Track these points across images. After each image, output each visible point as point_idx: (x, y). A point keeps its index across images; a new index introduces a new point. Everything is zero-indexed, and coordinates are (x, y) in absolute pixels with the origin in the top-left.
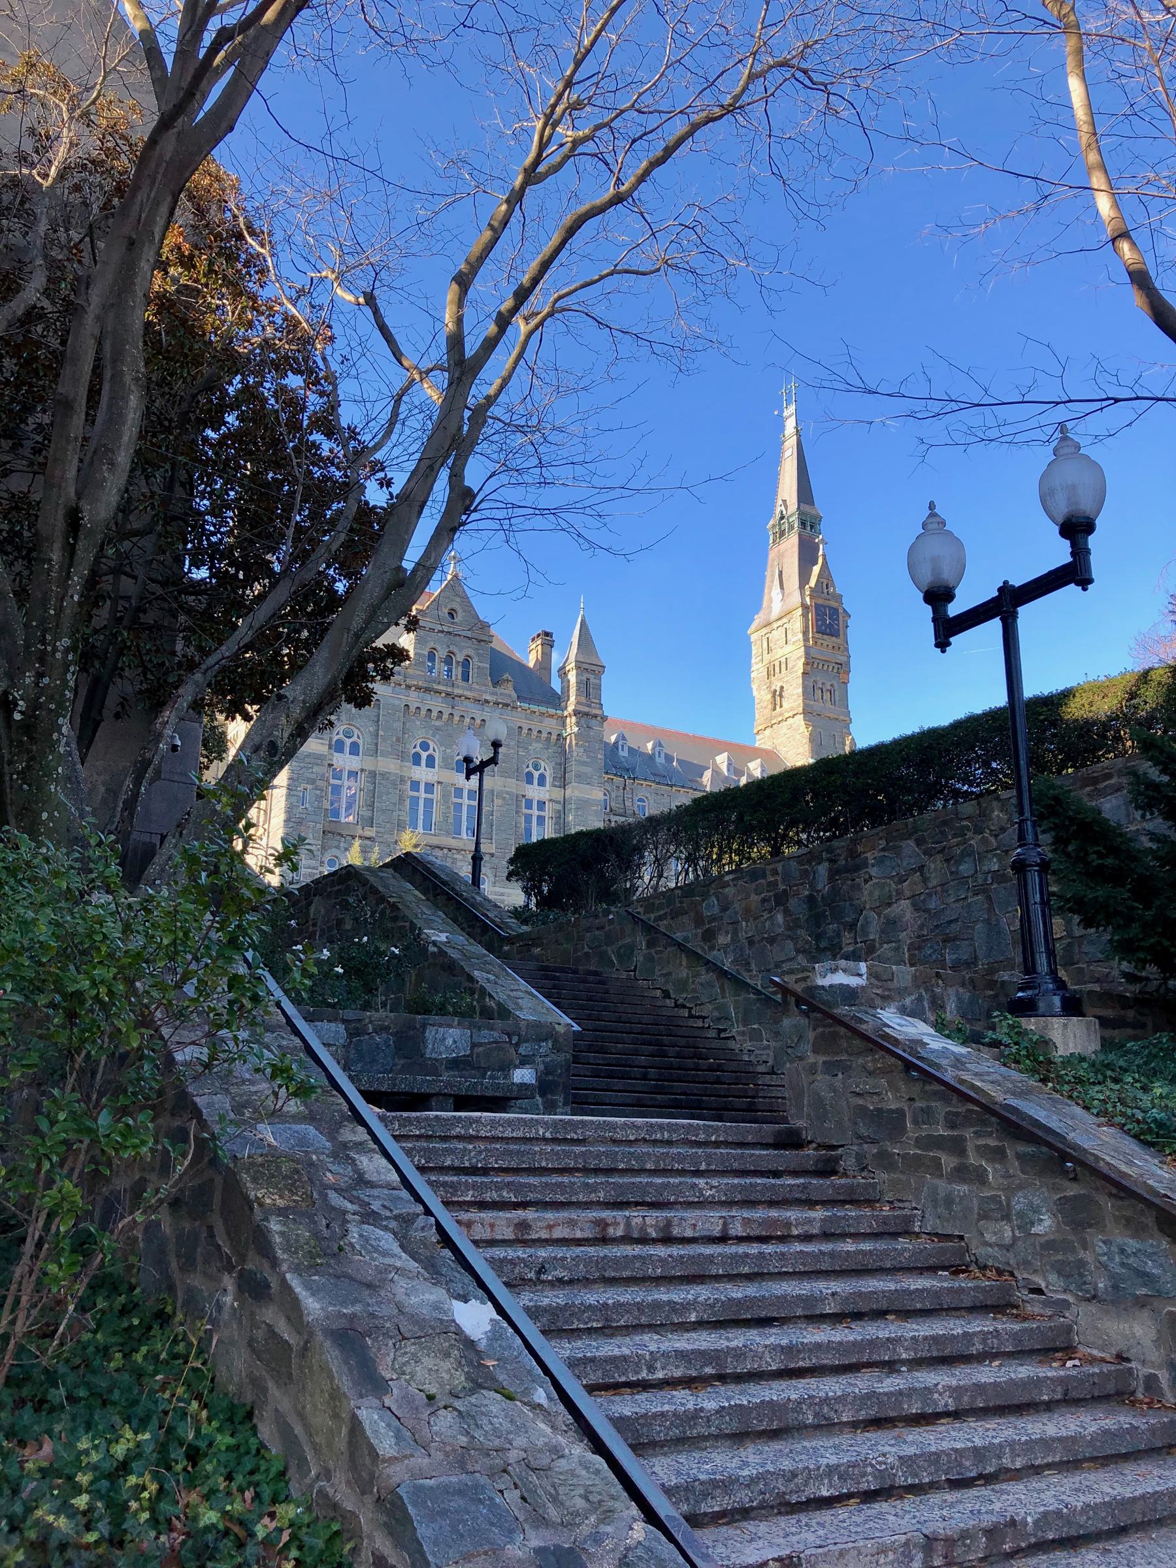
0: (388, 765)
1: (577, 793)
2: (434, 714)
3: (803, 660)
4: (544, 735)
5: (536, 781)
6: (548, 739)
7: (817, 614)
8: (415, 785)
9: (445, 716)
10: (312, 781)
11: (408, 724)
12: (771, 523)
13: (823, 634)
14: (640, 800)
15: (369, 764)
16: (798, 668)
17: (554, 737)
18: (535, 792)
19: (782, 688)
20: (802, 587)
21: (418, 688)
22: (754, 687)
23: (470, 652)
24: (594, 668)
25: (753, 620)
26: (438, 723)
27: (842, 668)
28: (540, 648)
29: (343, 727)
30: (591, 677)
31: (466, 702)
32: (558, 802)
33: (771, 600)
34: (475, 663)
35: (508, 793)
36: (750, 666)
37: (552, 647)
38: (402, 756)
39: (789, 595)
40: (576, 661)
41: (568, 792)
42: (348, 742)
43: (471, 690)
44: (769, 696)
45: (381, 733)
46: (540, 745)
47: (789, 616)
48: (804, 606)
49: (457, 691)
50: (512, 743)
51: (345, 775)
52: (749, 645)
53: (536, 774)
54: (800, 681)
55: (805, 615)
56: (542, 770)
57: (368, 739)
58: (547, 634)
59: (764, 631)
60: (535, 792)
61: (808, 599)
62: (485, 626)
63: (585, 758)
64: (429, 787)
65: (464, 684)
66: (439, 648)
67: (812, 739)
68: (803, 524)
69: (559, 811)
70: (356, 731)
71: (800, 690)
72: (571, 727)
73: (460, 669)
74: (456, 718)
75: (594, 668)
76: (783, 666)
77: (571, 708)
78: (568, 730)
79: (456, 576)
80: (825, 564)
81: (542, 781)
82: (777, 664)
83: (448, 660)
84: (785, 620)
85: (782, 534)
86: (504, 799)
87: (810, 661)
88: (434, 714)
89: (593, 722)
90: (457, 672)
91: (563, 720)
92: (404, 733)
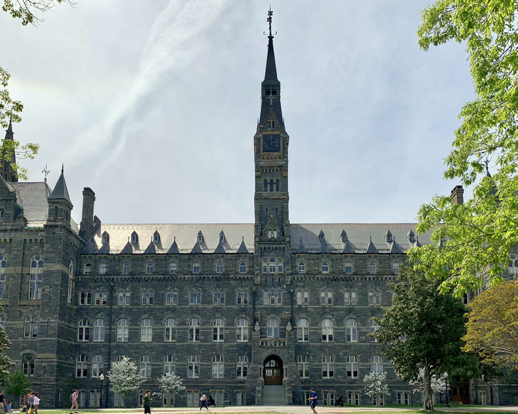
35: (16, 274)
46: (38, 247)
63: (51, 250)
86: (14, 277)
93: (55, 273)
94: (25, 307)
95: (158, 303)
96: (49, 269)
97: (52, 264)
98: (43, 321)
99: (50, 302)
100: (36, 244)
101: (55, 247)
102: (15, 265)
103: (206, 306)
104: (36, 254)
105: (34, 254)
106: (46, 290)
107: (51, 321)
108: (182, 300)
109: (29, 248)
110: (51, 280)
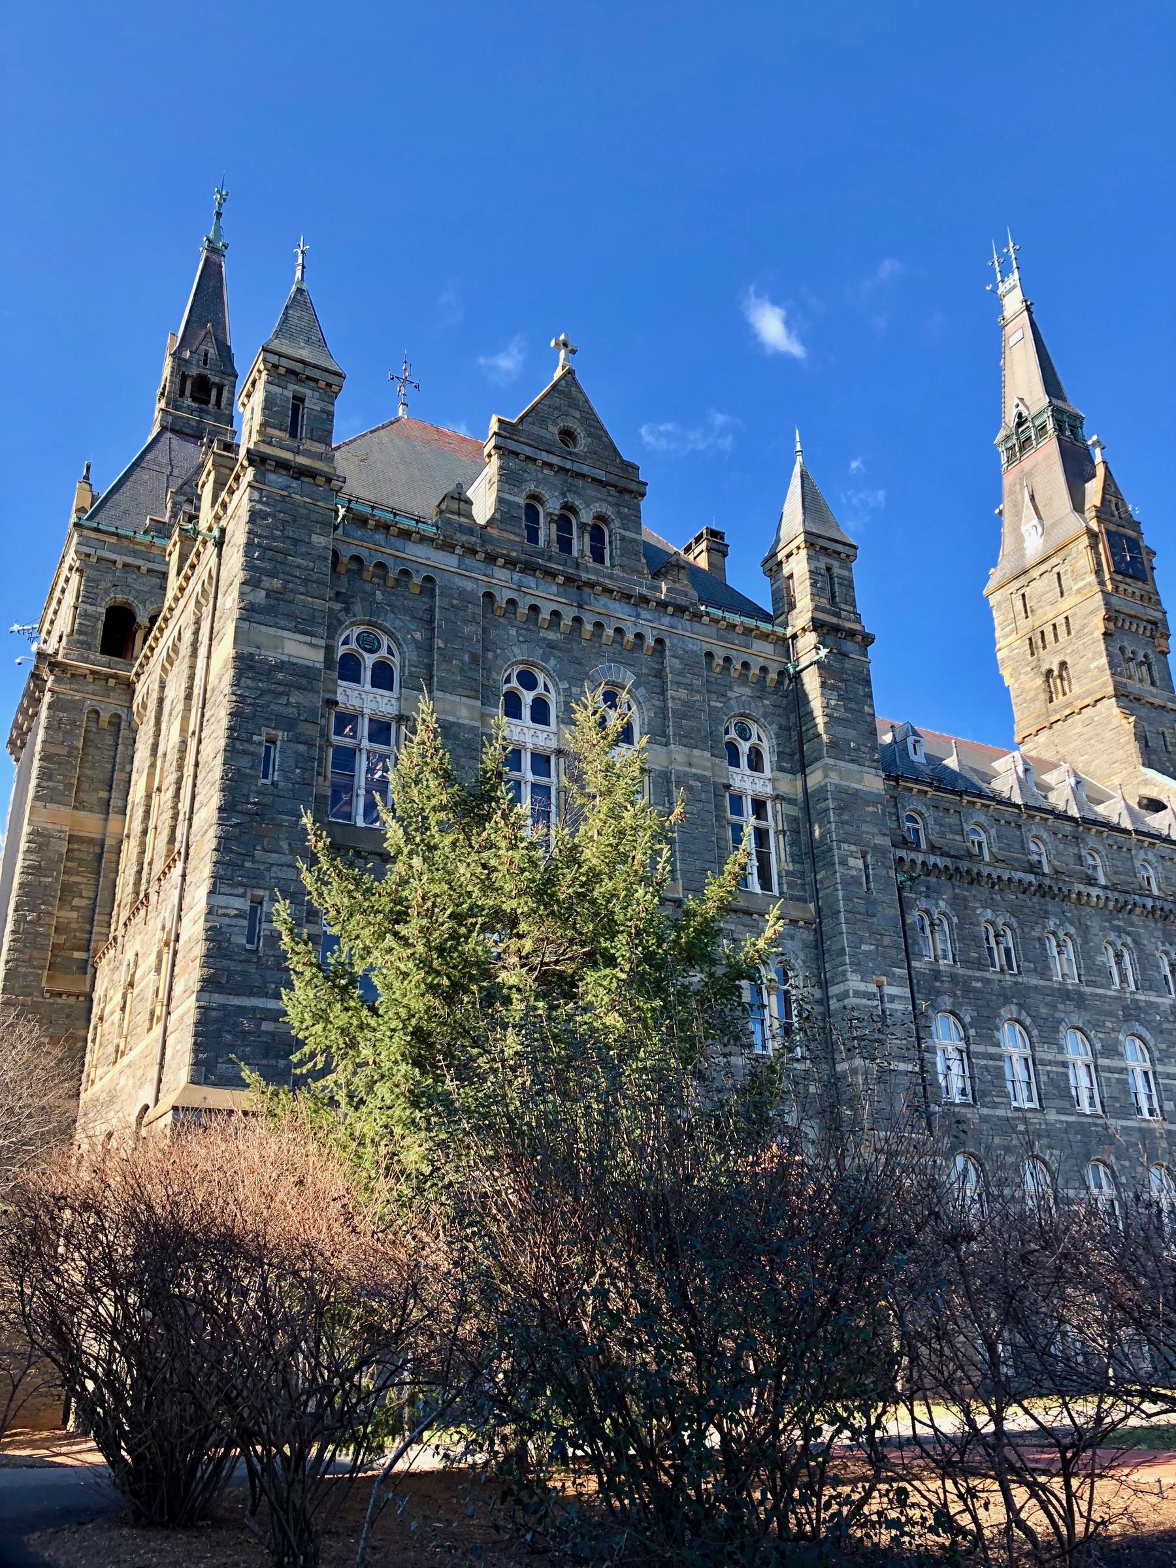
1: (834, 778)
2: (545, 615)
3: (1102, 613)
4: (754, 670)
5: (744, 761)
6: (761, 681)
7: (1111, 546)
9: (567, 621)
10: (288, 724)
11: (493, 634)
12: (1001, 435)
13: (1125, 575)
14: (911, 819)
16: (1098, 625)
17: (773, 676)
18: (745, 781)
19: (1063, 665)
20: (1078, 505)
21: (511, 563)
22: (1006, 673)
23: (609, 512)
24: (839, 548)
25: (987, 578)
26: (552, 636)
27: (1158, 628)
28: (704, 554)
29: (357, 630)
30: (836, 564)
31: (604, 600)
32: (791, 801)
33: (1020, 539)
34: (615, 531)
35: (698, 778)
36: (993, 642)
37: (725, 555)
38: (484, 694)
39: (1053, 526)
40: (806, 532)
41: (815, 779)
42: (369, 660)
43: (611, 577)
44: (1039, 681)
45: (439, 643)
46: (747, 691)
47: (1063, 552)
48: (1093, 535)
49: (585, 576)
50: (698, 682)
52: (989, 611)
54: (1102, 646)
55: (1093, 546)
56: (754, 739)
57: (412, 654)
58: (714, 533)
59: (1016, 584)
60: (745, 781)
61: (1094, 525)
65: (598, 566)
66: (546, 495)
67: (1137, 737)
68: (1059, 427)
69: (795, 819)
70: (385, 640)
71: (1104, 660)
72: (808, 649)
74: (589, 627)
75: (839, 548)
76: (1062, 630)
77: (802, 614)
78: (804, 662)
79: (570, 372)
80: (1108, 474)
81: (756, 763)
82: (1048, 630)
83: (563, 523)
84: (1054, 561)
85: (1025, 444)
87: (1111, 616)
88: (545, 615)
89: (849, 646)
90: (580, 544)
91: (786, 645)
92: (486, 649)
93: (868, 803)
94: (746, 918)
95: (1035, 970)
96: (843, 783)
97: (854, 767)
98: (862, 987)
99: (874, 915)
100: (743, 679)
101: (853, 705)
102: (689, 740)
103: (1153, 999)
104: (742, 715)
105: (735, 716)
106: (852, 862)
107: (888, 990)
108: (1093, 972)
109: (722, 689)
110: (864, 828)
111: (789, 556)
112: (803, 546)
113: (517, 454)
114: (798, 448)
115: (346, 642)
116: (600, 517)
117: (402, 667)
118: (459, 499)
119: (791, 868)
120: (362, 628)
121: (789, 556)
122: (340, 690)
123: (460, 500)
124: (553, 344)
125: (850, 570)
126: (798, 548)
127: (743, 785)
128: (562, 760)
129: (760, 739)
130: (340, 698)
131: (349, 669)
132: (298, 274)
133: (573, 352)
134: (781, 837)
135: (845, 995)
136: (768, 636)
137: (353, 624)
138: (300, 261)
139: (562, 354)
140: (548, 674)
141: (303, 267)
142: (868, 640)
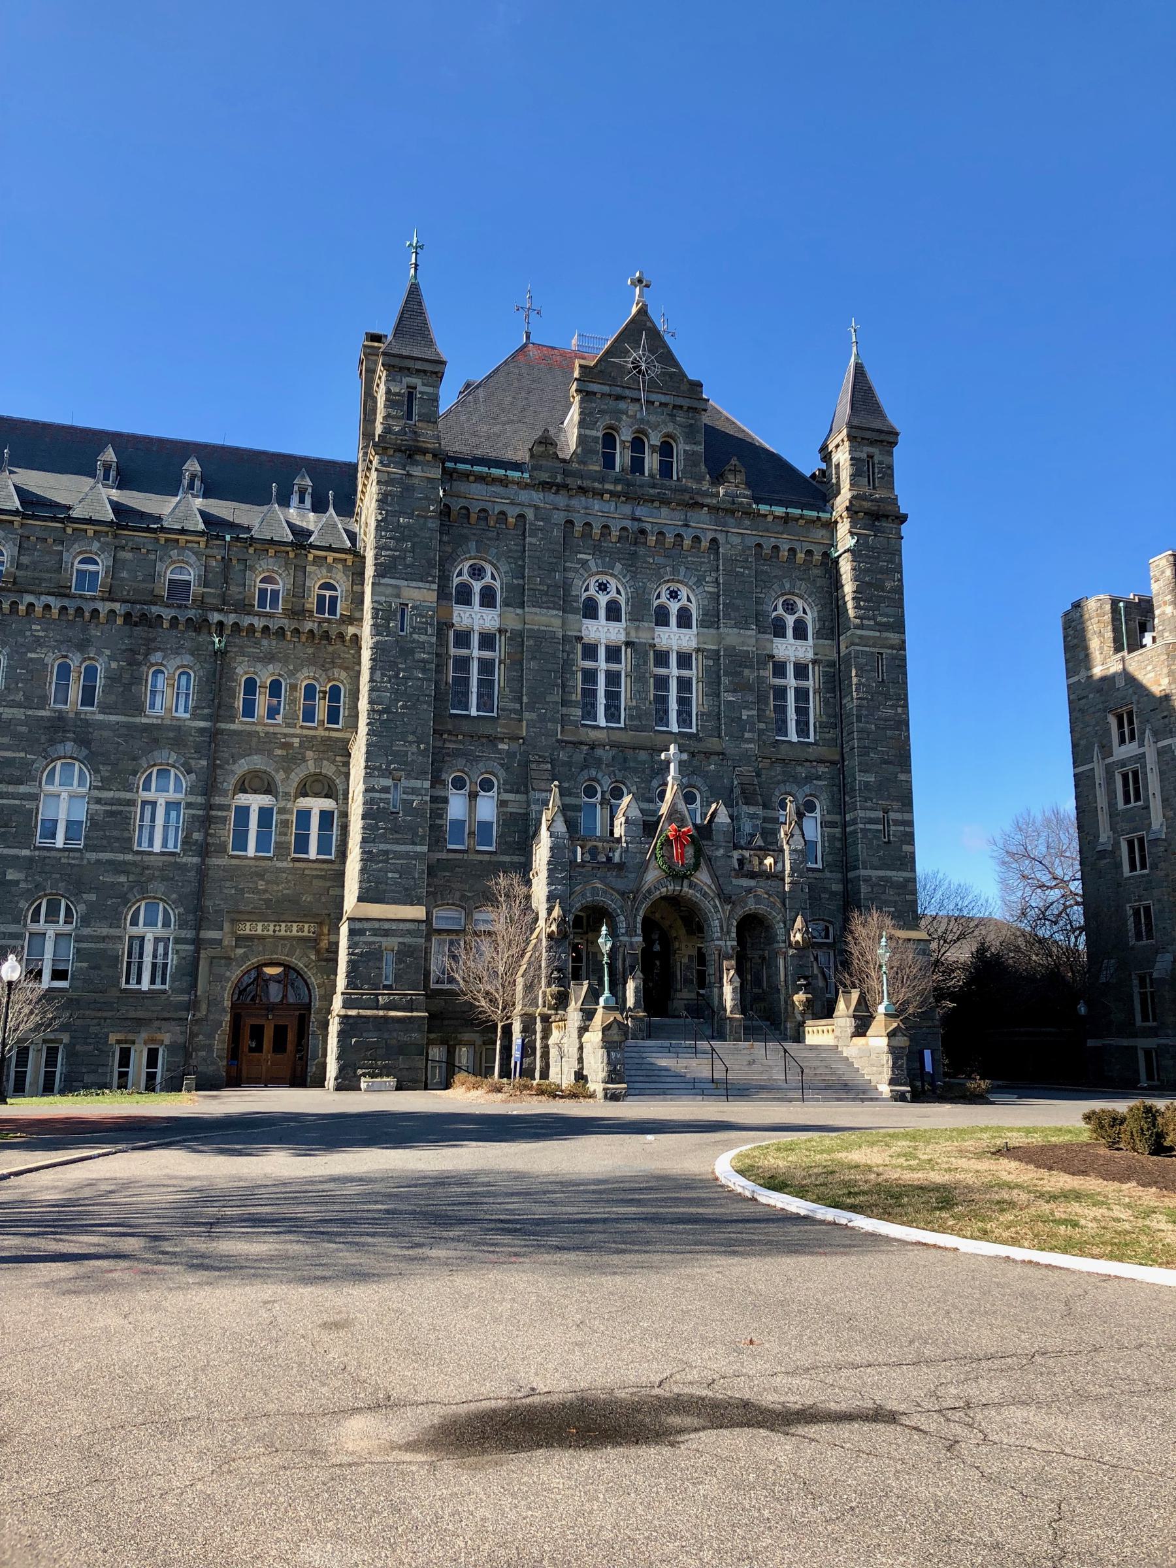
0: (545, 619)
5: (790, 632)
8: (590, 651)
15: (513, 622)
18: (789, 649)
29: (467, 565)
34: (680, 448)
40: (850, 426)
42: (477, 586)
51: (475, 640)
53: (790, 620)
56: (800, 613)
60: (789, 649)
62: (696, 387)
64: (613, 654)
70: (489, 569)
73: (656, 457)
79: (643, 311)
81: (800, 632)
83: (637, 444)
111: (837, 446)
112: (846, 439)
113: (595, 394)
114: (854, 340)
115: (460, 574)
116: (668, 435)
117: (502, 588)
118: (546, 442)
119: (824, 719)
120: (472, 562)
121: (837, 446)
122: (455, 614)
123: (546, 444)
124: (629, 282)
125: (891, 454)
126: (843, 441)
127: (787, 652)
128: (629, 650)
129: (805, 612)
130: (455, 620)
131: (464, 596)
132: (412, 271)
133: (647, 286)
134: (817, 695)
135: (854, 822)
136: (814, 522)
137: (462, 561)
138: (413, 261)
139: (638, 289)
140: (618, 580)
141: (416, 265)
142: (903, 519)
